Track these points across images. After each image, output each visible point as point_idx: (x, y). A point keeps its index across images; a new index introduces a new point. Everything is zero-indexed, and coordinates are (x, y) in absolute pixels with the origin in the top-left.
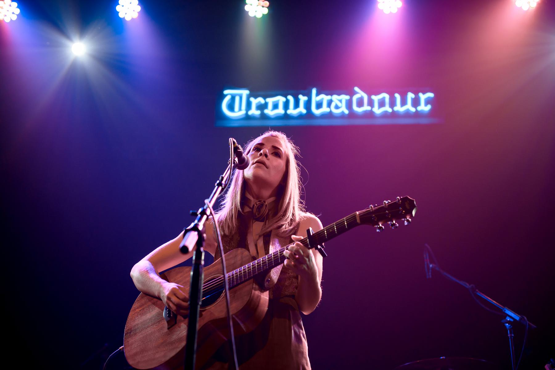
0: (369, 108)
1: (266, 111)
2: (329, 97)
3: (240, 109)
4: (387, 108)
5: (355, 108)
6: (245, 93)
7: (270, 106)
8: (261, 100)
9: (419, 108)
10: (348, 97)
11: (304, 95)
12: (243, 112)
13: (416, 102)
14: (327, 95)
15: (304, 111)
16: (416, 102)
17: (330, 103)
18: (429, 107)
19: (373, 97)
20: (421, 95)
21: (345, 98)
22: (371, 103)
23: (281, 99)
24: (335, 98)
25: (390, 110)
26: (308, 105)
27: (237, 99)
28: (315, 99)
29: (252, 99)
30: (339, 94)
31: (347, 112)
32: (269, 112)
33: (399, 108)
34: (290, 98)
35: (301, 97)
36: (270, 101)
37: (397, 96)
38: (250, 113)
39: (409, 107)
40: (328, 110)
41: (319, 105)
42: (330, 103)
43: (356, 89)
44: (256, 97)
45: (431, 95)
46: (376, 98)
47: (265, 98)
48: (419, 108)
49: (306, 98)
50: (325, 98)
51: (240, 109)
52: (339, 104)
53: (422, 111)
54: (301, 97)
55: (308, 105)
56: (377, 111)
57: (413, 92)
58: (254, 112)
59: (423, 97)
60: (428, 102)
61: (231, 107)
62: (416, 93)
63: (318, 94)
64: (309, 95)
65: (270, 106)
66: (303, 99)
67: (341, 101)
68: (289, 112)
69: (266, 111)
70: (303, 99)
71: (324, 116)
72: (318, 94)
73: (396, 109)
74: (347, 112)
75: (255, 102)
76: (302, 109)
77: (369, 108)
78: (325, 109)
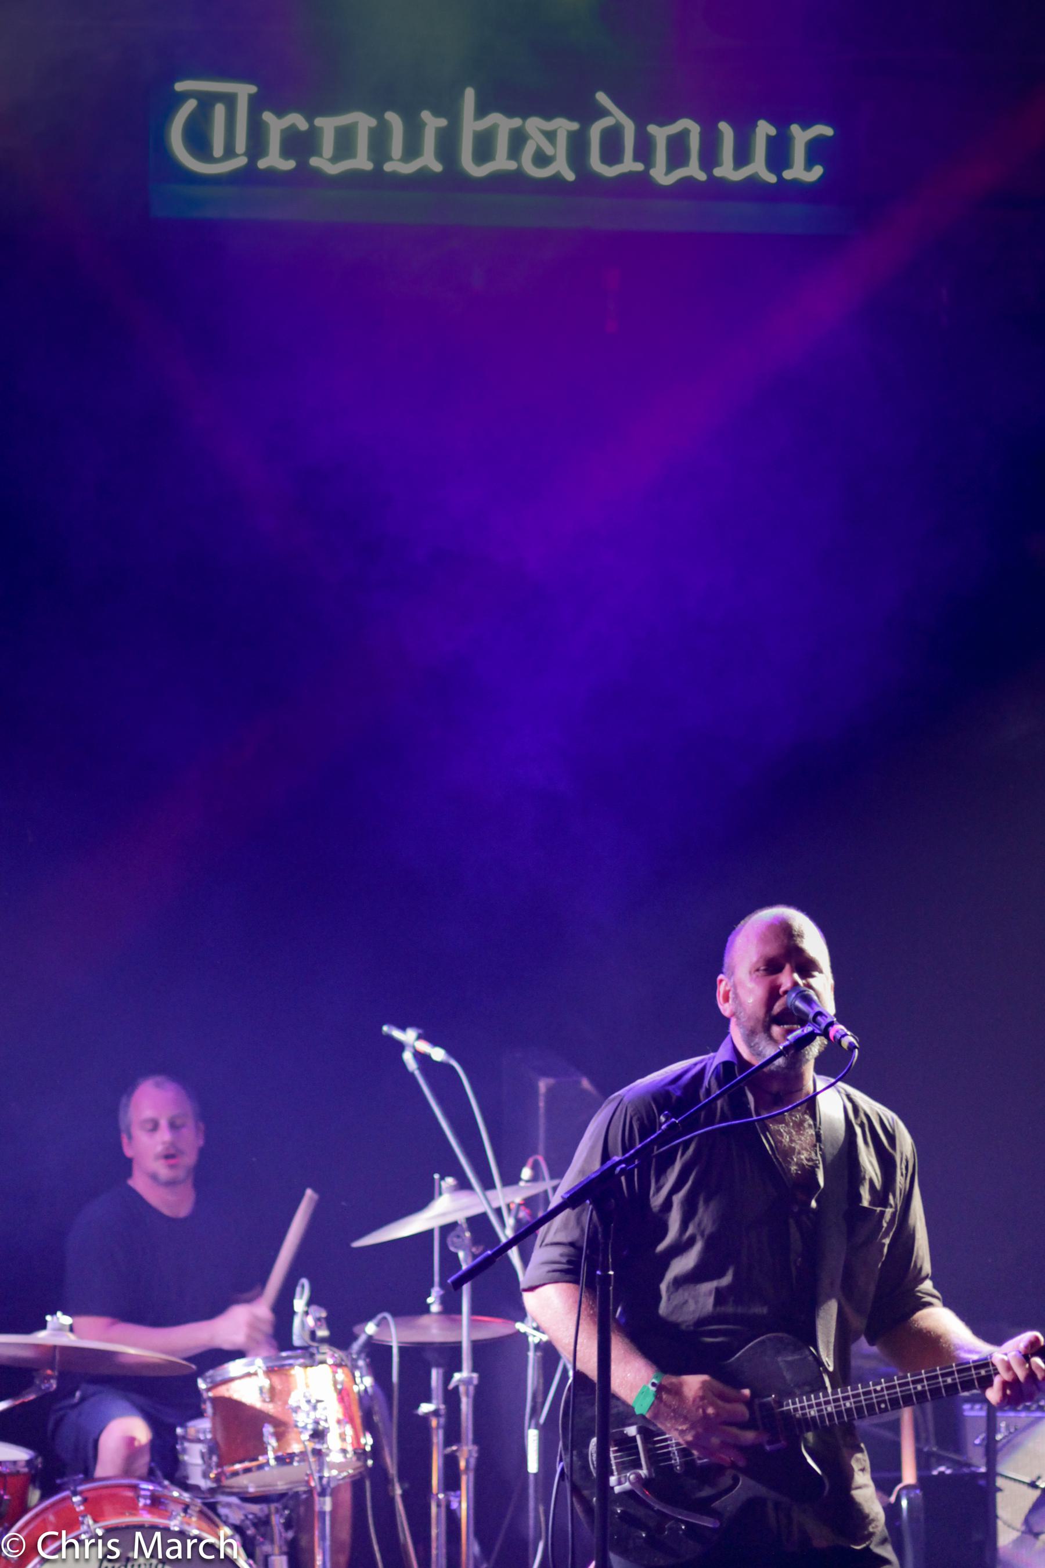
0: (639, 167)
1: (314, 162)
2: (516, 122)
3: (230, 152)
4: (693, 170)
5: (596, 163)
6: (244, 91)
7: (328, 145)
8: (297, 120)
9: (788, 175)
10: (575, 126)
11: (437, 113)
12: (239, 162)
13: (779, 155)
14: (510, 112)
15: (437, 167)
16: (779, 155)
17: (518, 140)
18: (817, 172)
19: (652, 129)
20: (795, 128)
21: (564, 126)
22: (644, 150)
23: (363, 122)
24: (534, 125)
25: (702, 176)
26: (448, 146)
27: (219, 111)
28: (470, 126)
29: (268, 116)
30: (548, 116)
31: (570, 176)
32: (324, 163)
33: (727, 171)
34: (393, 119)
35: (426, 115)
36: (328, 125)
37: (725, 128)
38: (262, 164)
39: (758, 167)
40: (512, 166)
41: (484, 149)
42: (518, 140)
43: (602, 98)
44: (280, 113)
45: (828, 131)
46: (660, 134)
47: (310, 119)
48: (788, 175)
49: (443, 122)
50: (503, 124)
51: (230, 152)
52: (549, 150)
53: (796, 183)
54: (426, 115)
55: (448, 146)
56: (662, 176)
57: (772, 121)
58: (274, 160)
59: (801, 136)
60: (816, 151)
61: (199, 142)
62: (782, 122)
63: (481, 111)
64: (451, 110)
65: (328, 145)
66: (432, 123)
67: (551, 136)
68: (388, 167)
69: (314, 162)
70: (432, 123)
71: (501, 182)
72: (481, 111)
73: (718, 172)
74: (570, 176)
75: (276, 125)
76: (429, 161)
77: (639, 167)
78: (501, 162)
